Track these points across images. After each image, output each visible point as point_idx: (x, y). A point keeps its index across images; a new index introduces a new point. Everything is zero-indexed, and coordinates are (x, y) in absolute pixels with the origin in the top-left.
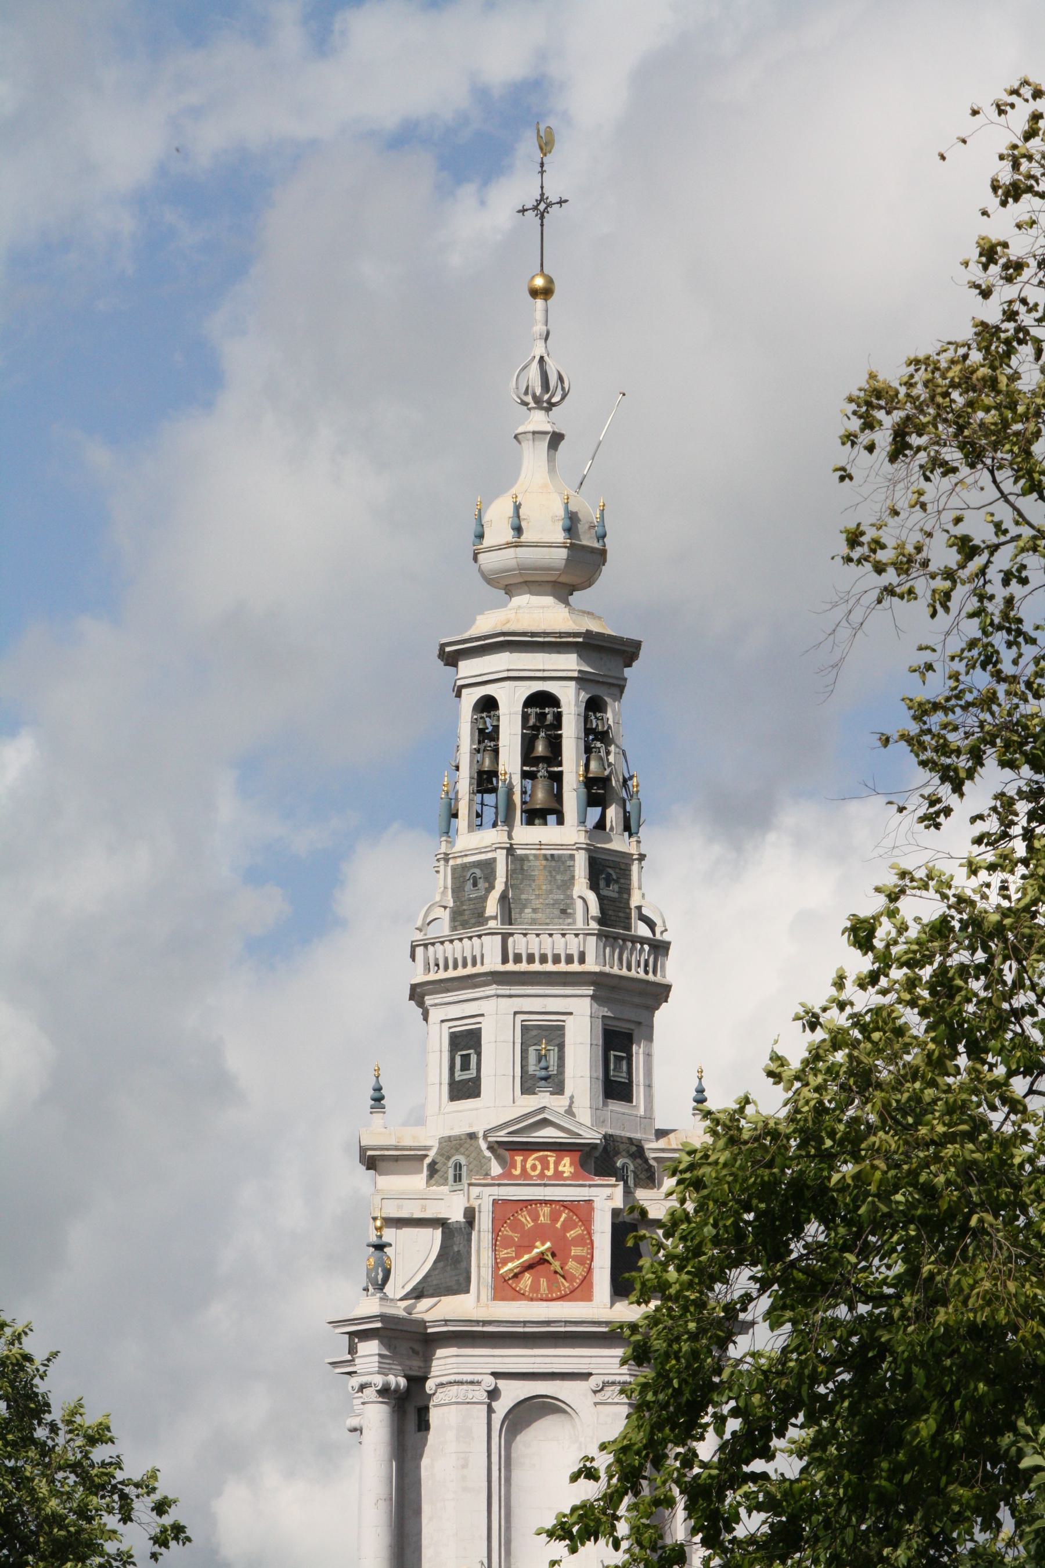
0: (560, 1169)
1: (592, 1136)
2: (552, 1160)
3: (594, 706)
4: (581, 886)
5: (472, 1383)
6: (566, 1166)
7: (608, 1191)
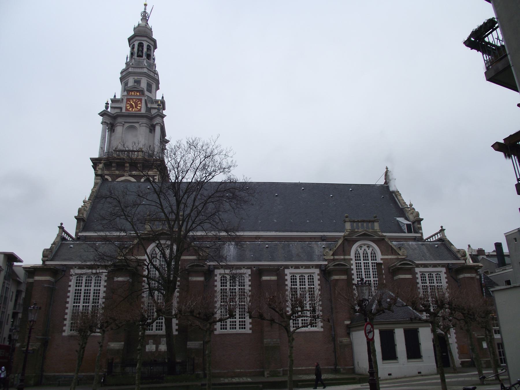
0: (137, 94)
2: (136, 93)
3: (148, 46)
5: (120, 123)
6: (138, 94)
7: (144, 97)
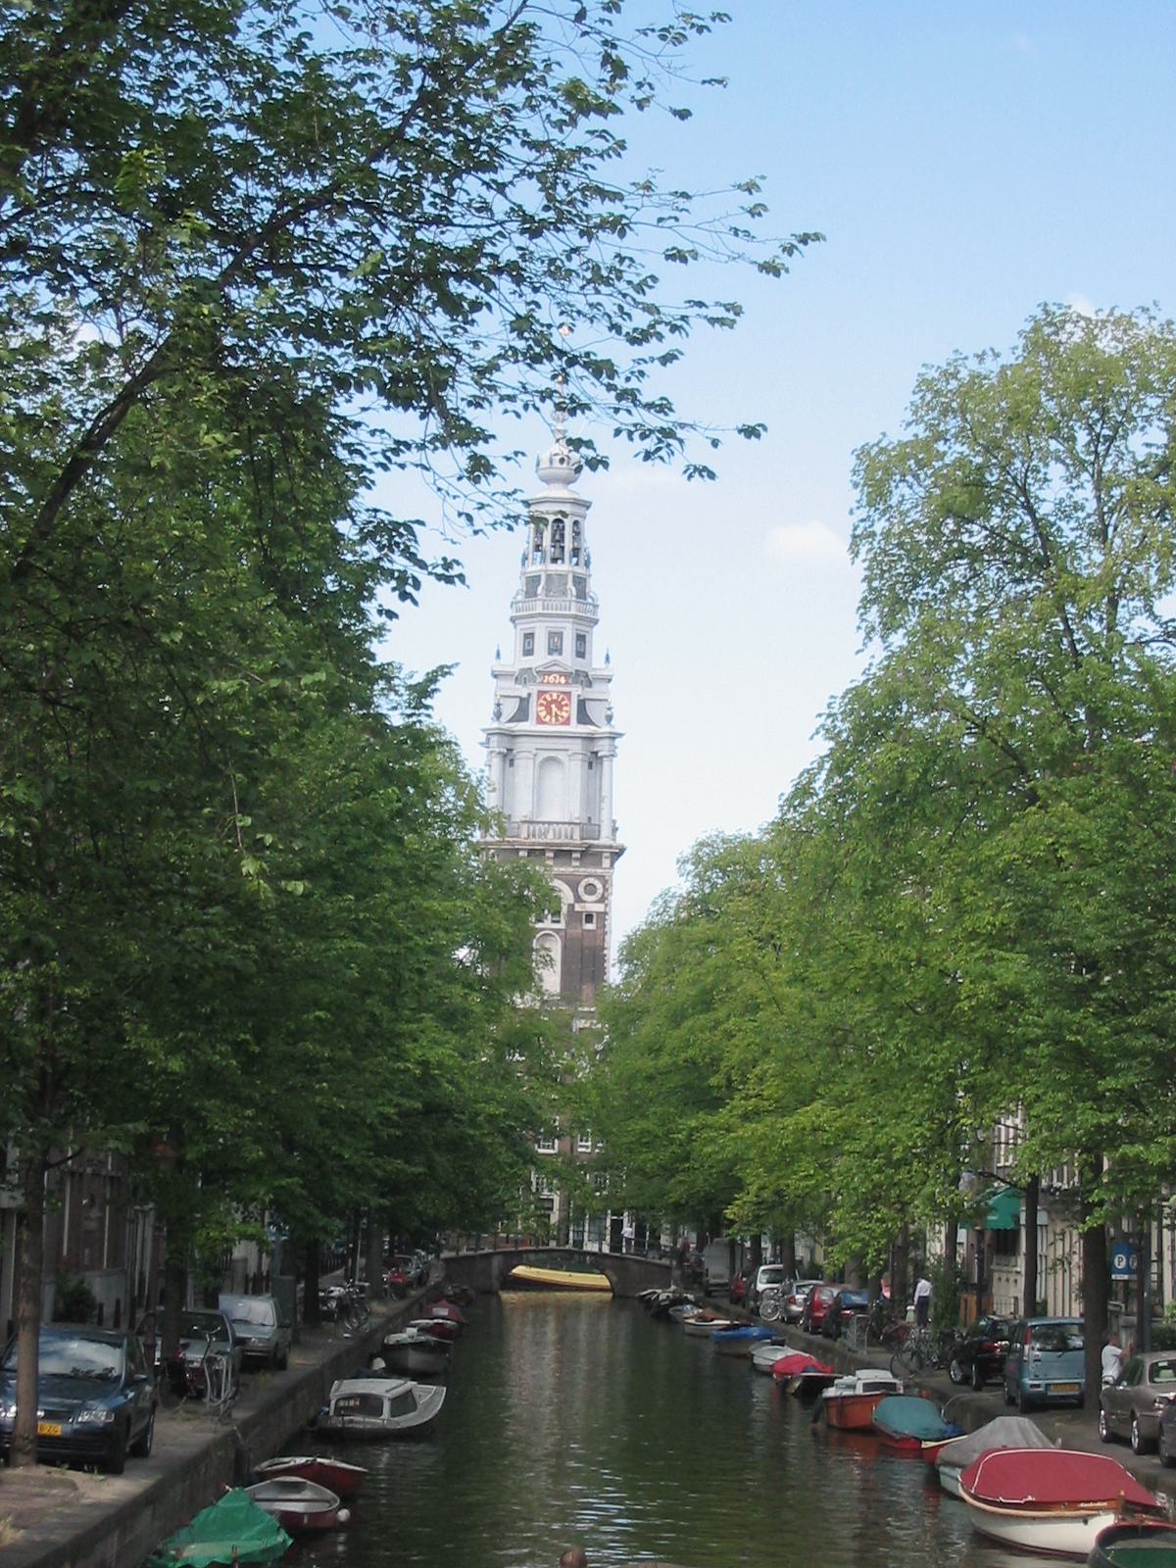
1: (516, 669)
3: (576, 523)
4: (570, 585)
6: (563, 680)
